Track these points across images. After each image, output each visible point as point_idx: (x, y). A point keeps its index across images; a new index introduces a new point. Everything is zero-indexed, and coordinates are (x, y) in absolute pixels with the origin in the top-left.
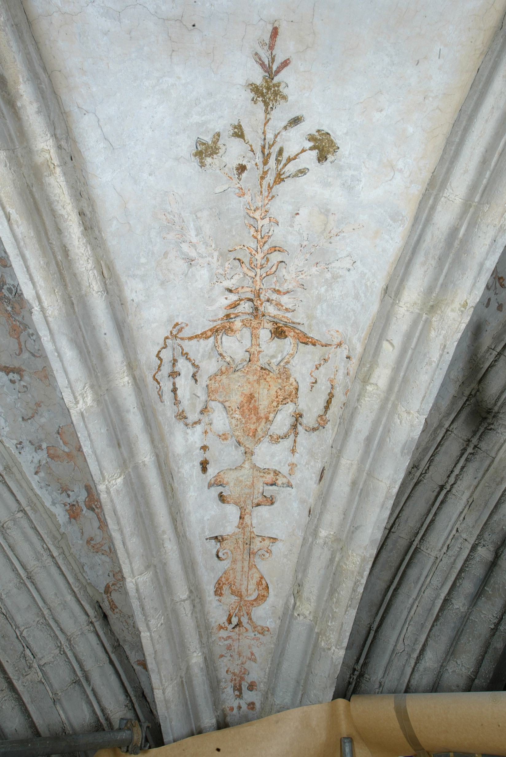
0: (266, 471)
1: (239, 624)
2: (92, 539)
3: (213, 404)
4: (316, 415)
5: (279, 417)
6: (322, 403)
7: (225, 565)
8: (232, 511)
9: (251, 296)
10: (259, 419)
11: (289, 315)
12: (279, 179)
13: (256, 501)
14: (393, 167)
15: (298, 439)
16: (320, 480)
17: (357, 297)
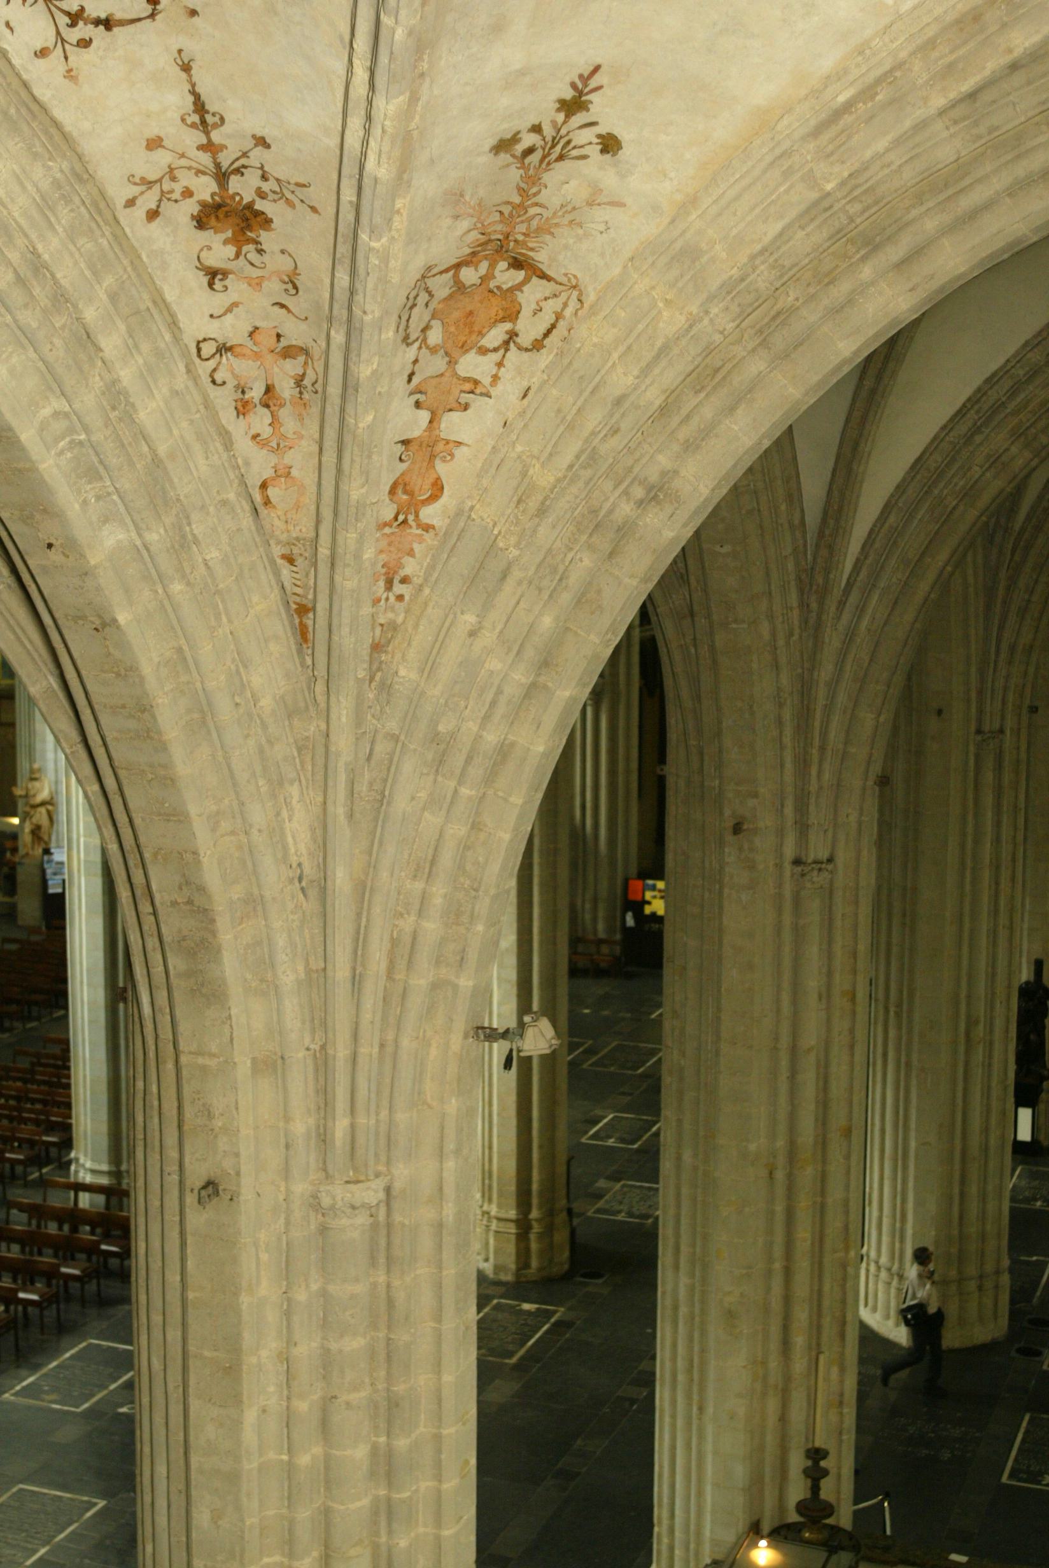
0: (467, 380)
1: (405, 522)
2: (258, 435)
3: (433, 323)
4: (533, 338)
5: (493, 332)
6: (542, 329)
7: (404, 466)
8: (424, 416)
9: (501, 237)
10: (471, 333)
11: (531, 254)
12: (561, 158)
13: (448, 407)
14: (665, 176)
15: (508, 354)
16: (525, 396)
17: (602, 255)
